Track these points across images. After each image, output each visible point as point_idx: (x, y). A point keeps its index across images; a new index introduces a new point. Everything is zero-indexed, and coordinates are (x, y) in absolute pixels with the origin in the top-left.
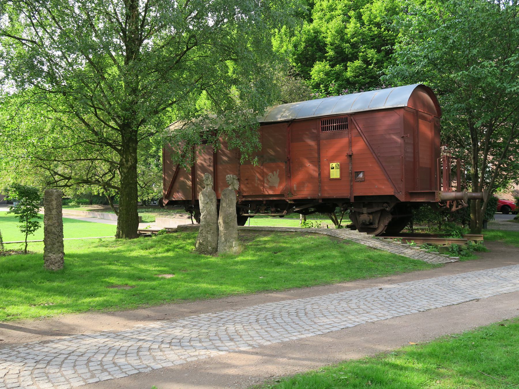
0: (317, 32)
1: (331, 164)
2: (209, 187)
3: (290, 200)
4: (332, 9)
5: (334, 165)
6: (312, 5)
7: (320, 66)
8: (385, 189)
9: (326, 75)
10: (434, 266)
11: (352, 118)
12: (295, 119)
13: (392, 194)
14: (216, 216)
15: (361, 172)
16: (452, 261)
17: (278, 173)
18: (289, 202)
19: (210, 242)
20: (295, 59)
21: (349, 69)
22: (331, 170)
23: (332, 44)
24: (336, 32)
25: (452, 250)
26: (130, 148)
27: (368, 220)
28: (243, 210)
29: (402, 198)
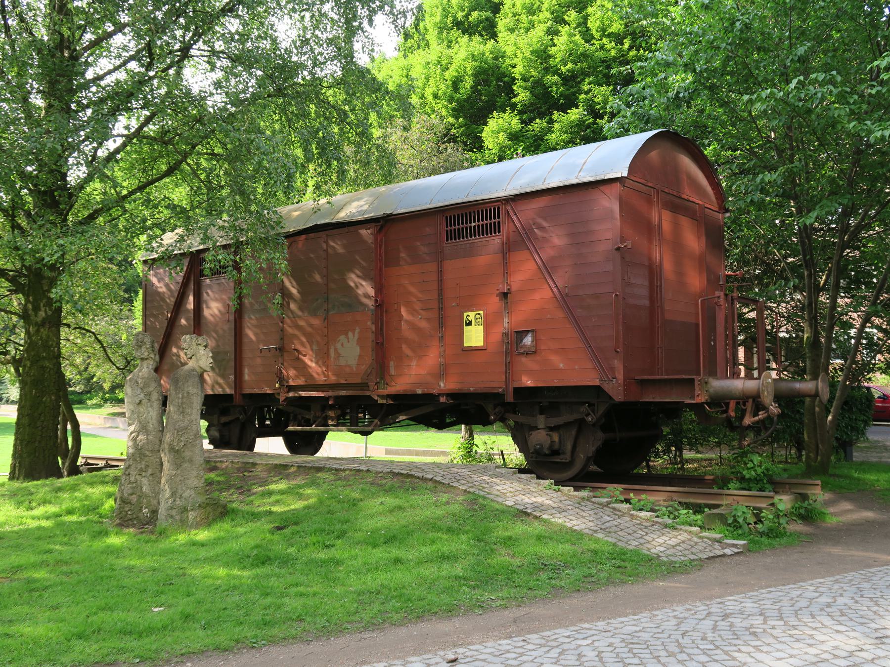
0: (499, 56)
1: (465, 314)
2: (145, 363)
3: (382, 397)
4: (531, 11)
5: (472, 315)
6: (496, 9)
7: (500, 121)
8: (583, 374)
9: (510, 139)
10: (672, 569)
11: (509, 208)
12: (391, 215)
13: (597, 382)
14: (99, 439)
15: (528, 332)
16: (728, 551)
17: (357, 336)
18: (381, 401)
19: (147, 496)
20: (453, 109)
21: (556, 126)
22: (466, 328)
23: (525, 79)
24: (532, 52)
25: (735, 521)
26: (44, 281)
27: (547, 444)
28: (295, 419)
29: (616, 391)
